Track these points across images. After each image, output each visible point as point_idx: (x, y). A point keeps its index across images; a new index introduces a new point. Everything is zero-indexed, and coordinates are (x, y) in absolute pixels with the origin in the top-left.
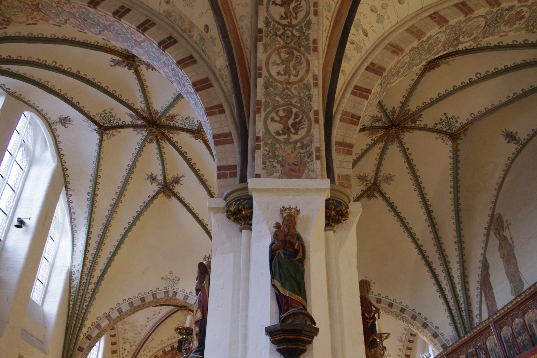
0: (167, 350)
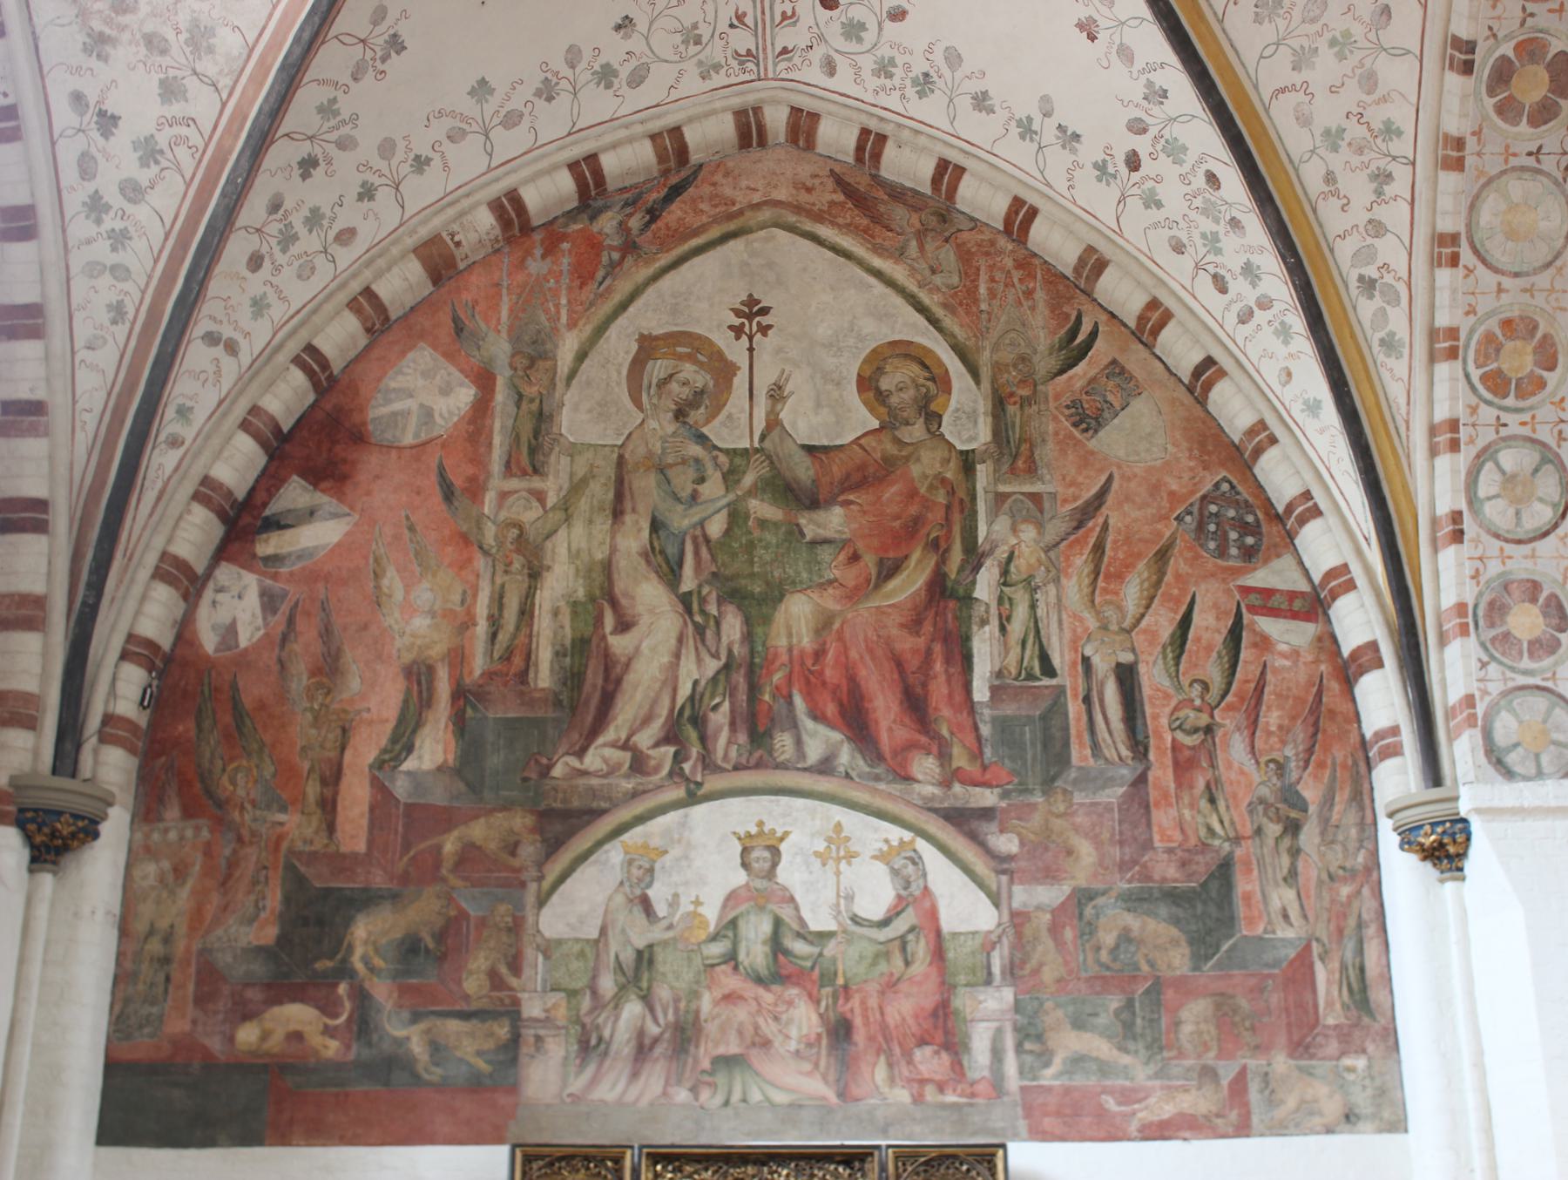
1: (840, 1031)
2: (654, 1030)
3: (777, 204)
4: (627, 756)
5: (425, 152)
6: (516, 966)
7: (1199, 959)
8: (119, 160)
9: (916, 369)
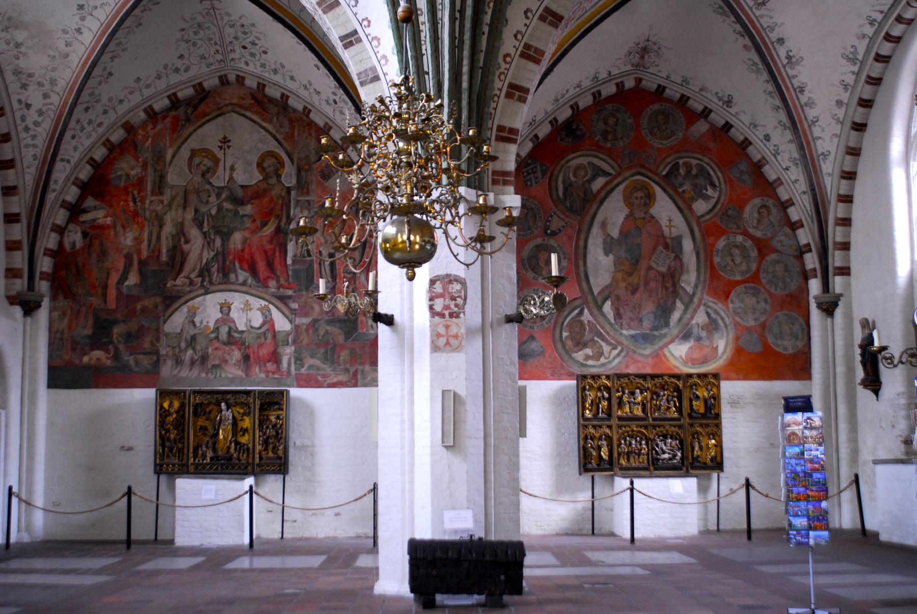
0: (157, 107)
1: (246, 358)
2: (196, 357)
3: (233, 104)
4: (187, 281)
5: (122, 98)
6: (158, 340)
7: (346, 339)
8: (32, 116)
9: (274, 160)
